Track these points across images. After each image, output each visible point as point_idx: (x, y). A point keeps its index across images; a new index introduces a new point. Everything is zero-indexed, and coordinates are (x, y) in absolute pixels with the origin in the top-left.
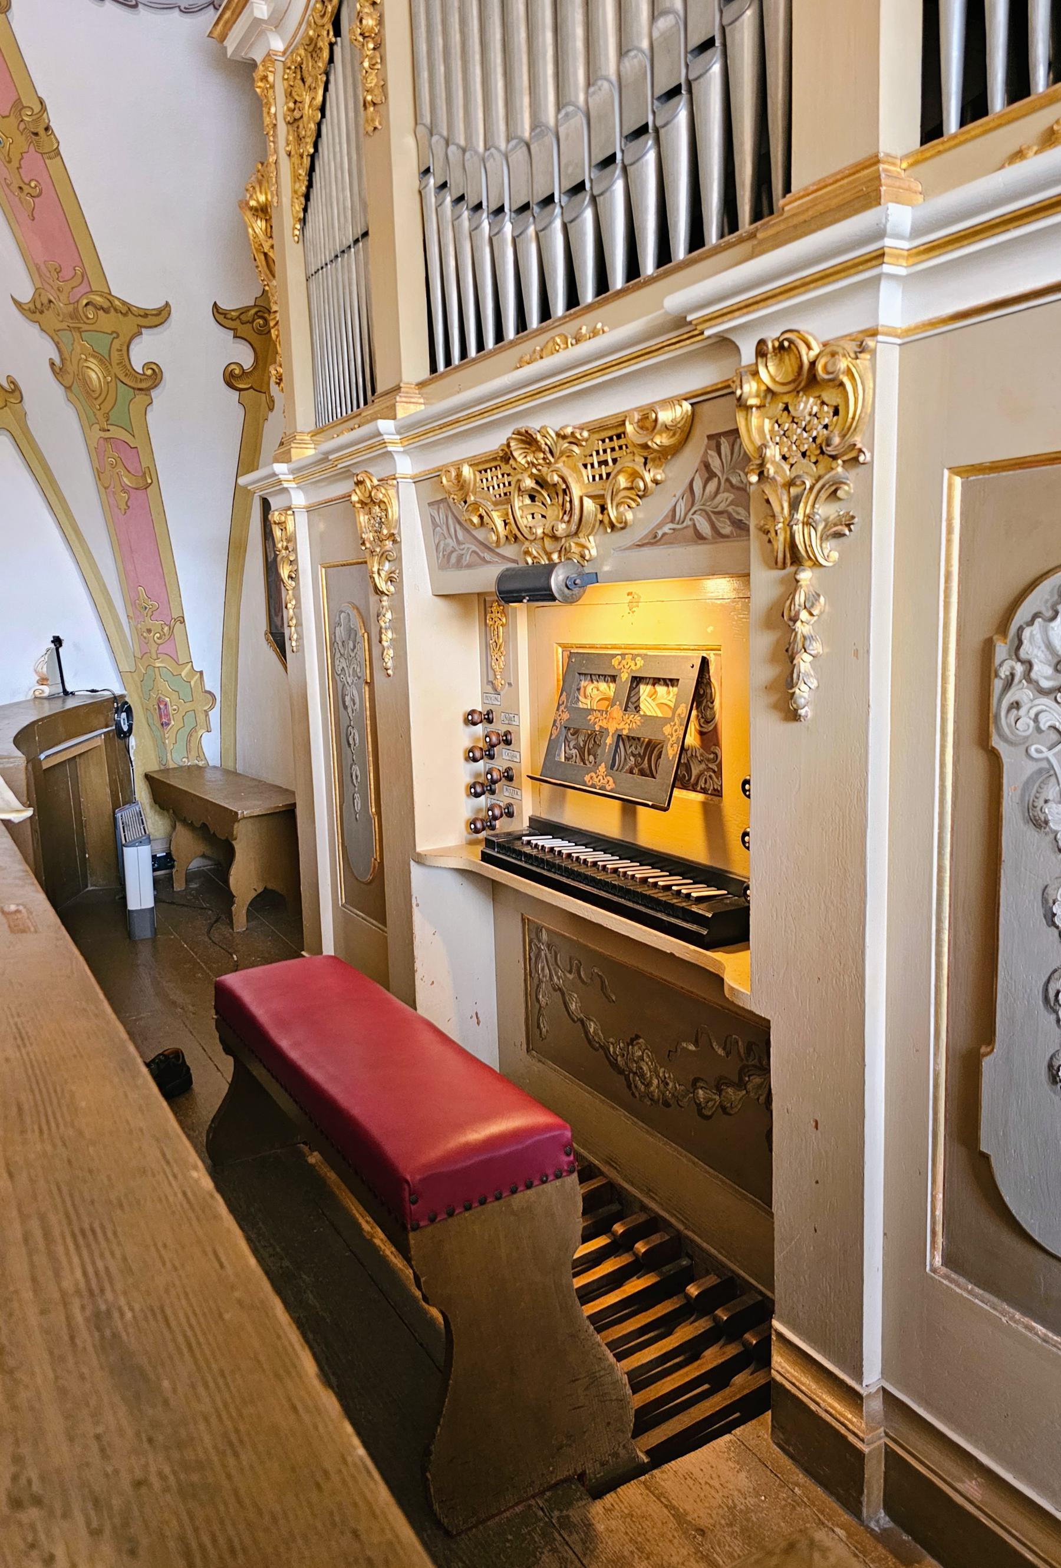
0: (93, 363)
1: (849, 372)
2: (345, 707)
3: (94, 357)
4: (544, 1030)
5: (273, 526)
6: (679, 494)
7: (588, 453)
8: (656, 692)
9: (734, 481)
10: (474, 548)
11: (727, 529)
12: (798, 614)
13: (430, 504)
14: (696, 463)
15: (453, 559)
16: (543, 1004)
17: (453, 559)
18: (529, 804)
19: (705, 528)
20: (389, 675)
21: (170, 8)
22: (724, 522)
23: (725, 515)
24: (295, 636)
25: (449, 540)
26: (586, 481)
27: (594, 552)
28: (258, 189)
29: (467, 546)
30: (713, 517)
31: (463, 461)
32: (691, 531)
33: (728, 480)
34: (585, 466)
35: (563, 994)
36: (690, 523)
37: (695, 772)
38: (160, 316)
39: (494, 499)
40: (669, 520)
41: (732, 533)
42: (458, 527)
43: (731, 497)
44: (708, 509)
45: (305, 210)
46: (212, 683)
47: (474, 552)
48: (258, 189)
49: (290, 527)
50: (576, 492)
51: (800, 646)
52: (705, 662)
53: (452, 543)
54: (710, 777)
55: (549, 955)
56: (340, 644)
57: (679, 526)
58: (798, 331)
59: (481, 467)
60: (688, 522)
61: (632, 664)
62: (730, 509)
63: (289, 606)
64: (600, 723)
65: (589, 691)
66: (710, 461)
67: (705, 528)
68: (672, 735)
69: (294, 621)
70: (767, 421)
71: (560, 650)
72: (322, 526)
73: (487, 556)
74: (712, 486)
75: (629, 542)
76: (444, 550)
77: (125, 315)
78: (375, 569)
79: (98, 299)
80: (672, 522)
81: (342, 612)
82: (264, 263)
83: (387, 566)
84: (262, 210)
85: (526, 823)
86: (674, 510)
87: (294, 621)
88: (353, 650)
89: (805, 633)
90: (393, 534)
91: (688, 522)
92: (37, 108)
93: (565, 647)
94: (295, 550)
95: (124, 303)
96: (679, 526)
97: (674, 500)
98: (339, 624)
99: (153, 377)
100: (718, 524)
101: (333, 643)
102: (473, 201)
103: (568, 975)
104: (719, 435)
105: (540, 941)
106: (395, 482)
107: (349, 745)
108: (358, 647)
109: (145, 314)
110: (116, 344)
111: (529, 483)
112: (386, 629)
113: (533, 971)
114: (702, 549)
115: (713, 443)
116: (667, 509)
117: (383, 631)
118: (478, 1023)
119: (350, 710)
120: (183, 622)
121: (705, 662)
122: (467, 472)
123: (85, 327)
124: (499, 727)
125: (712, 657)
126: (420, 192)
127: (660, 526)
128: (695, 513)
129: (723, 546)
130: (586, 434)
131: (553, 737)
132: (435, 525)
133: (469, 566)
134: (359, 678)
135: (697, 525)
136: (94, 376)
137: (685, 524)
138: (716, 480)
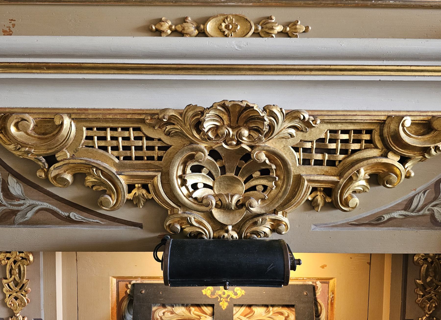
8: (252, 311)
10: (46, 205)
29: (29, 202)
31: (59, 112)
32: (428, 219)
39: (117, 161)
40: (403, 207)
60: (426, 211)
71: (114, 281)
73: (74, 215)
75: (341, 221)
80: (405, 209)
86: (411, 201)
91: (426, 211)
97: (413, 193)
127: (387, 211)
137: (421, 213)
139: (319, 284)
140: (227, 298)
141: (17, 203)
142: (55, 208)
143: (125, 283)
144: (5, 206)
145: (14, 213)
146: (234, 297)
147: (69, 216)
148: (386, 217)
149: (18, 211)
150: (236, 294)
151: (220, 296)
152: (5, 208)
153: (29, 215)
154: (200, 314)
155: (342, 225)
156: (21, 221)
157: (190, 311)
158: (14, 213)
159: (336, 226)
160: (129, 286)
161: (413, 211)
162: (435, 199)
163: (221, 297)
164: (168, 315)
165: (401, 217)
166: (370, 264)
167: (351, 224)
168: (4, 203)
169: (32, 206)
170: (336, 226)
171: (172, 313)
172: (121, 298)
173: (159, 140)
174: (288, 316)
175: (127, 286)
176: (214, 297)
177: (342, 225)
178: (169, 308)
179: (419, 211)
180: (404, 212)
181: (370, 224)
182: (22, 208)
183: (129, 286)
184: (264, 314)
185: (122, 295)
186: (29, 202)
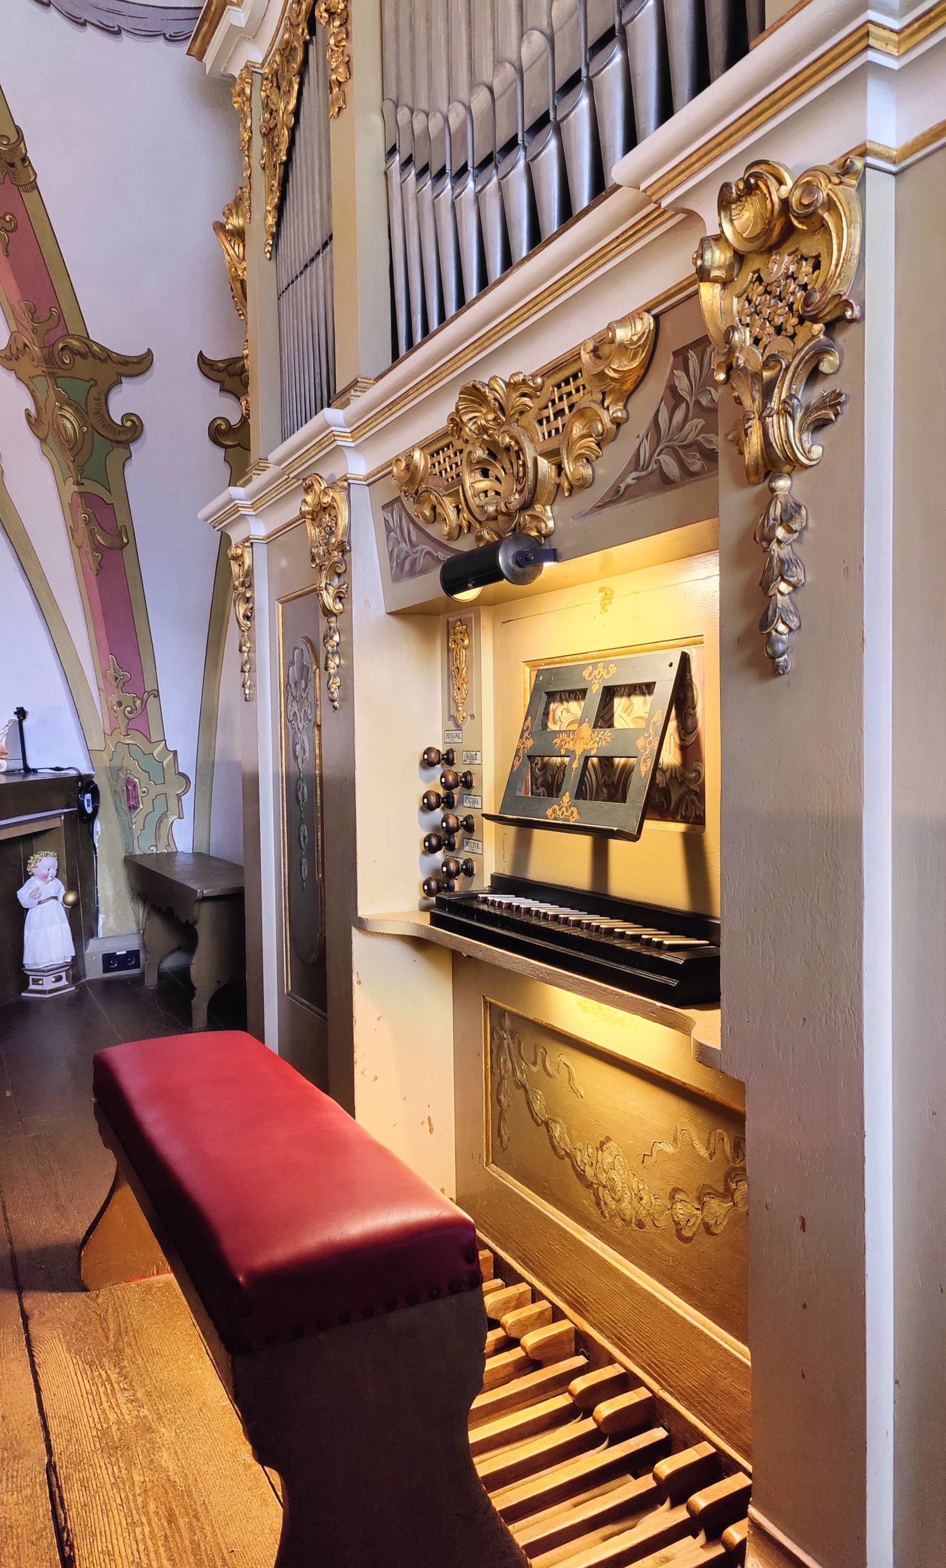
0: (68, 413)
1: (830, 205)
2: (296, 758)
3: (70, 406)
4: (505, 1138)
5: (232, 562)
6: (642, 433)
7: (542, 404)
8: (631, 704)
9: (704, 401)
10: (427, 548)
11: (696, 465)
12: (773, 529)
13: (384, 507)
15: (407, 567)
16: (505, 1106)
18: (491, 855)
19: (671, 467)
20: (335, 708)
21: (153, 35)
22: (694, 457)
23: (695, 447)
24: (248, 684)
25: (403, 545)
26: (541, 440)
27: (551, 524)
28: (234, 211)
33: (697, 403)
34: (540, 422)
35: (526, 1091)
36: (655, 466)
37: (674, 798)
38: (139, 365)
39: (446, 483)
41: (703, 467)
42: (411, 527)
45: (278, 224)
46: (187, 764)
47: (428, 553)
48: (234, 211)
49: (248, 562)
50: (530, 453)
51: (776, 572)
52: (685, 660)
53: (405, 547)
54: (692, 801)
55: (511, 1045)
56: (293, 685)
57: (644, 473)
58: (766, 162)
59: (434, 448)
60: (654, 466)
61: (604, 673)
62: (700, 438)
63: (244, 648)
64: (567, 746)
65: (558, 713)
66: (677, 384)
67: (671, 467)
69: (248, 666)
70: (735, 300)
71: (528, 670)
72: (284, 563)
74: (679, 415)
76: (398, 557)
77: (104, 361)
78: (323, 585)
79: (75, 343)
80: (636, 470)
81: (295, 648)
82: (240, 291)
83: (336, 581)
84: (238, 234)
85: (487, 883)
86: (637, 454)
87: (248, 666)
88: (304, 690)
89: (782, 556)
90: (343, 542)
91: (654, 466)
92: (14, 138)
93: (531, 663)
94: (250, 586)
95: (103, 349)
96: (644, 473)
97: (638, 440)
98: (292, 663)
99: (133, 429)
100: (687, 460)
101: (287, 684)
102: (435, 168)
103: (532, 1067)
104: (686, 349)
105: (502, 1028)
106: (346, 484)
107: (298, 801)
108: (309, 686)
109: (125, 361)
110: (94, 393)
111: (480, 453)
112: (333, 654)
113: (495, 1066)
115: (681, 359)
117: (330, 656)
118: (431, 1131)
119: (300, 760)
120: (157, 696)
121: (685, 660)
122: (418, 456)
123: (62, 373)
124: (460, 768)
125: (692, 652)
126: (386, 173)
127: (622, 478)
130: (539, 380)
131: (515, 769)
132: (389, 529)
134: (310, 721)
136: (69, 425)
138: (684, 405)
142: (431, 550)
148: (623, 486)
155: (591, 511)
159: (587, 514)
161: (642, 471)
164: (565, 713)
165: (635, 481)
167: (598, 507)
170: (587, 514)
177: (591, 511)
179: (648, 467)
180: (635, 474)
181: (612, 502)
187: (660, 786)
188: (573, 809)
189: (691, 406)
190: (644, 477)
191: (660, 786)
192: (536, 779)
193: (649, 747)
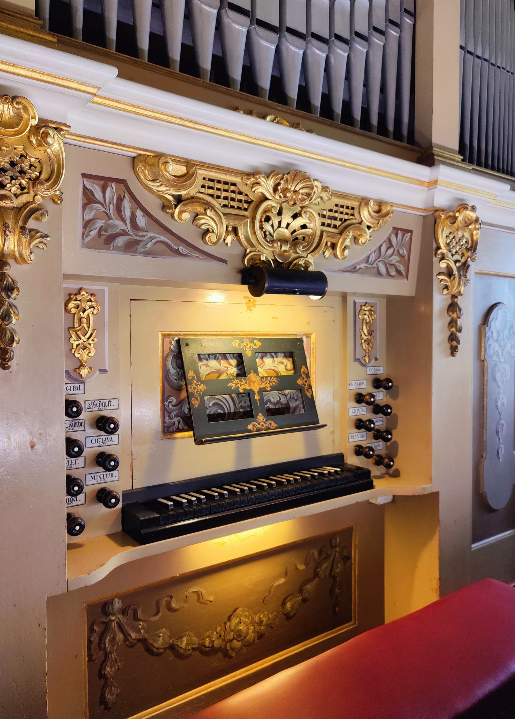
6: (373, 249)
9: (401, 252)
10: (162, 238)
11: (393, 273)
14: (385, 238)
17: (120, 241)
19: (383, 270)
22: (392, 269)
29: (150, 234)
30: (388, 266)
33: (398, 251)
41: (395, 275)
43: (398, 259)
44: (387, 261)
61: (252, 344)
62: (397, 264)
64: (243, 387)
66: (392, 239)
67: (383, 270)
68: (305, 385)
73: (182, 249)
74: (390, 251)
100: (390, 270)
114: (379, 280)
115: (395, 231)
116: (364, 256)
128: (379, 261)
129: (389, 281)
133: (148, 253)
135: (380, 269)
139: (305, 339)
140: (250, 348)
141: (141, 234)
142: (169, 242)
143: (169, 339)
144: (131, 235)
145: (137, 242)
146: (255, 347)
147: (178, 249)
149: (141, 241)
150: (255, 345)
151: (245, 346)
152: (131, 237)
153: (149, 245)
154: (228, 366)
156: (142, 250)
157: (220, 364)
158: (137, 242)
160: (173, 342)
162: (379, 257)
163: (246, 348)
166: (334, 321)
168: (131, 233)
169: (152, 238)
171: (207, 366)
172: (166, 354)
173: (246, 195)
174: (286, 366)
175: (170, 342)
176: (241, 347)
178: (205, 362)
182: (144, 239)
183: (173, 342)
184: (271, 364)
185: (167, 351)
186: (150, 234)
187: (283, 403)
188: (269, 421)
189: (396, 250)
190: (369, 268)
191: (283, 403)
192: (170, 413)
193: (306, 384)
